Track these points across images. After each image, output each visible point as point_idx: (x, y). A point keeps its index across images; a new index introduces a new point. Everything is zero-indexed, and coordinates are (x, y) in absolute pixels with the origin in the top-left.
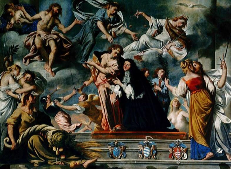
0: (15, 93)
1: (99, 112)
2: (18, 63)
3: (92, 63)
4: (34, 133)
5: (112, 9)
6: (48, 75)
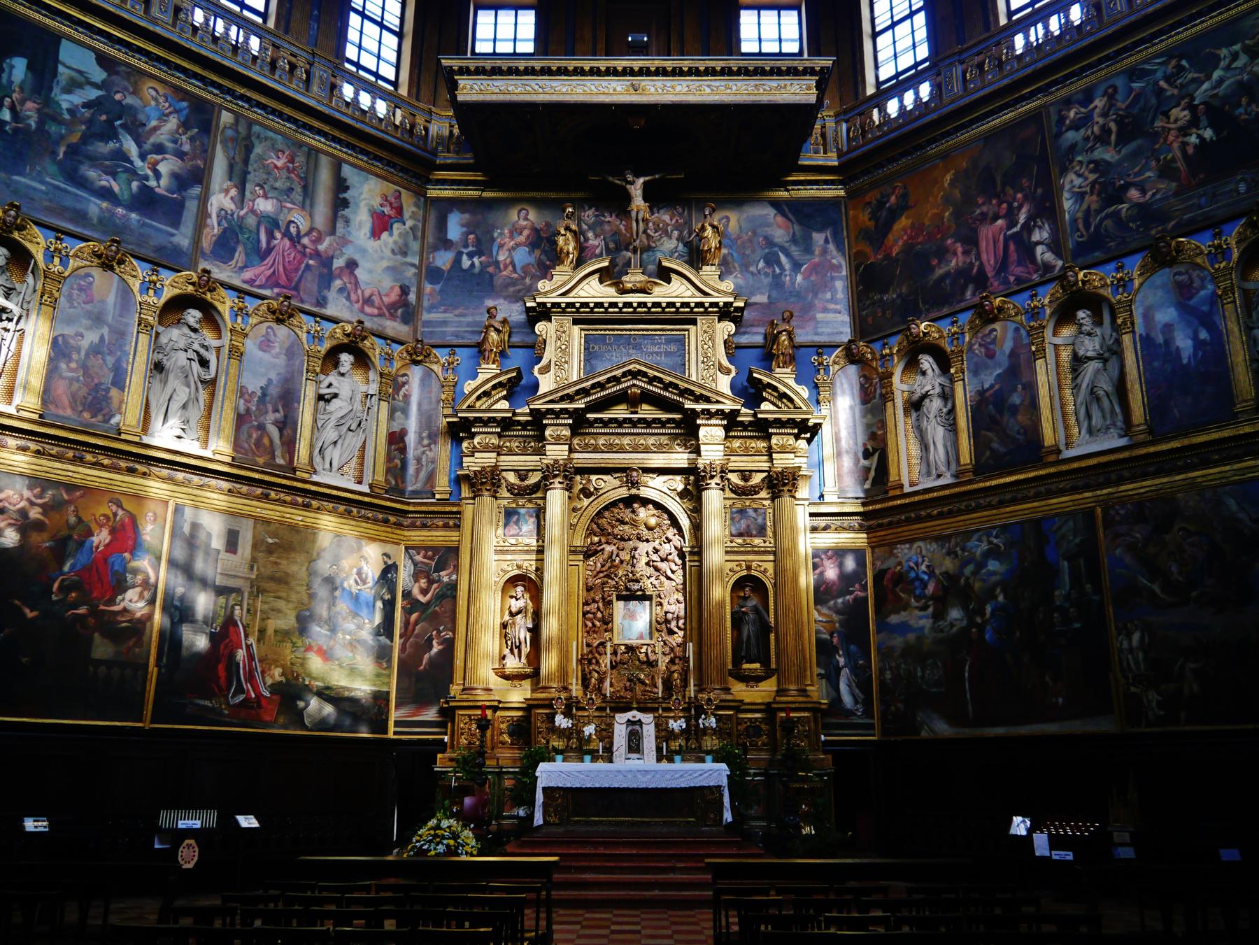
0: (1080, 187)
1: (1178, 168)
2: (1079, 158)
3: (1160, 124)
4: (1107, 217)
5: (1174, 62)
6: (1112, 157)
